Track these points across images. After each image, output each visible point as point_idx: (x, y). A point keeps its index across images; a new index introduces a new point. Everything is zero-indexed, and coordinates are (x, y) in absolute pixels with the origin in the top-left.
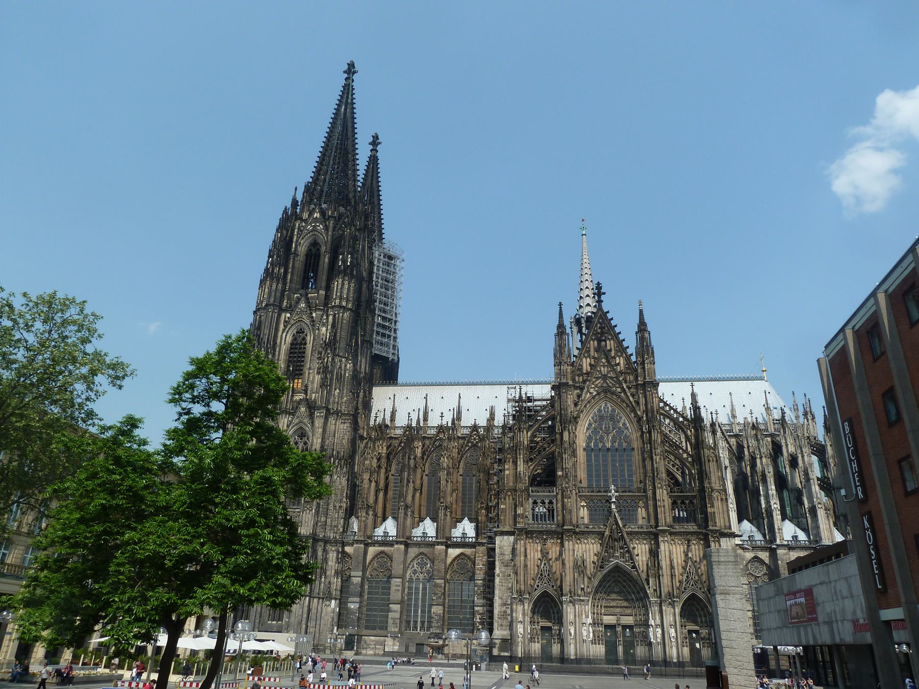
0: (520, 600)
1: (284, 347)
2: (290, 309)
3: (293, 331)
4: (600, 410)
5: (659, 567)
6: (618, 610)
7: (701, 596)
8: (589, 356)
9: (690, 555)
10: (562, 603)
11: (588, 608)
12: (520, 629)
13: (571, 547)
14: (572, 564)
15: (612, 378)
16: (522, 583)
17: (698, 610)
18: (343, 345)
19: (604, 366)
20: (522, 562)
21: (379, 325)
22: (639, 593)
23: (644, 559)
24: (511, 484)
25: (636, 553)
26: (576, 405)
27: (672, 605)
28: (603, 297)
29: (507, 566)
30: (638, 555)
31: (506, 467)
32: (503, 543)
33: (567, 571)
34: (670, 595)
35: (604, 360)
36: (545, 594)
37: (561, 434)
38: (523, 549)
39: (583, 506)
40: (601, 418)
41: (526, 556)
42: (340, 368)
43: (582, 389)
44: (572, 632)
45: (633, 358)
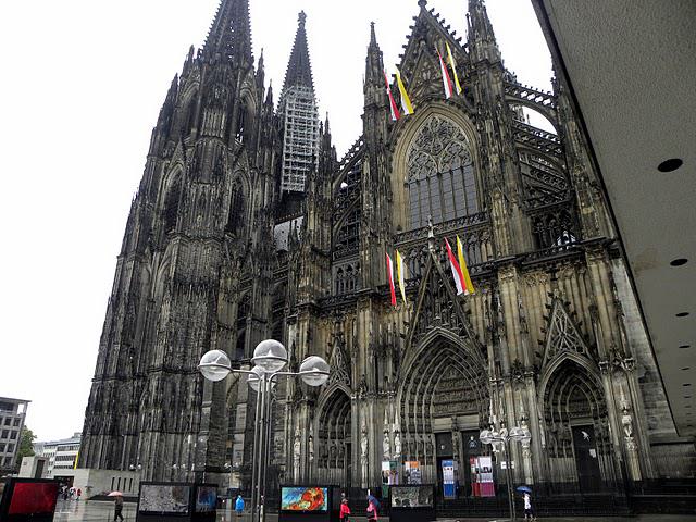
1: (164, 192)
2: (169, 157)
3: (172, 175)
4: (426, 129)
6: (456, 407)
7: (580, 361)
11: (394, 408)
12: (297, 449)
13: (368, 318)
17: (588, 391)
18: (206, 173)
21: (294, 164)
33: (362, 356)
38: (305, 334)
42: (203, 194)
44: (364, 447)
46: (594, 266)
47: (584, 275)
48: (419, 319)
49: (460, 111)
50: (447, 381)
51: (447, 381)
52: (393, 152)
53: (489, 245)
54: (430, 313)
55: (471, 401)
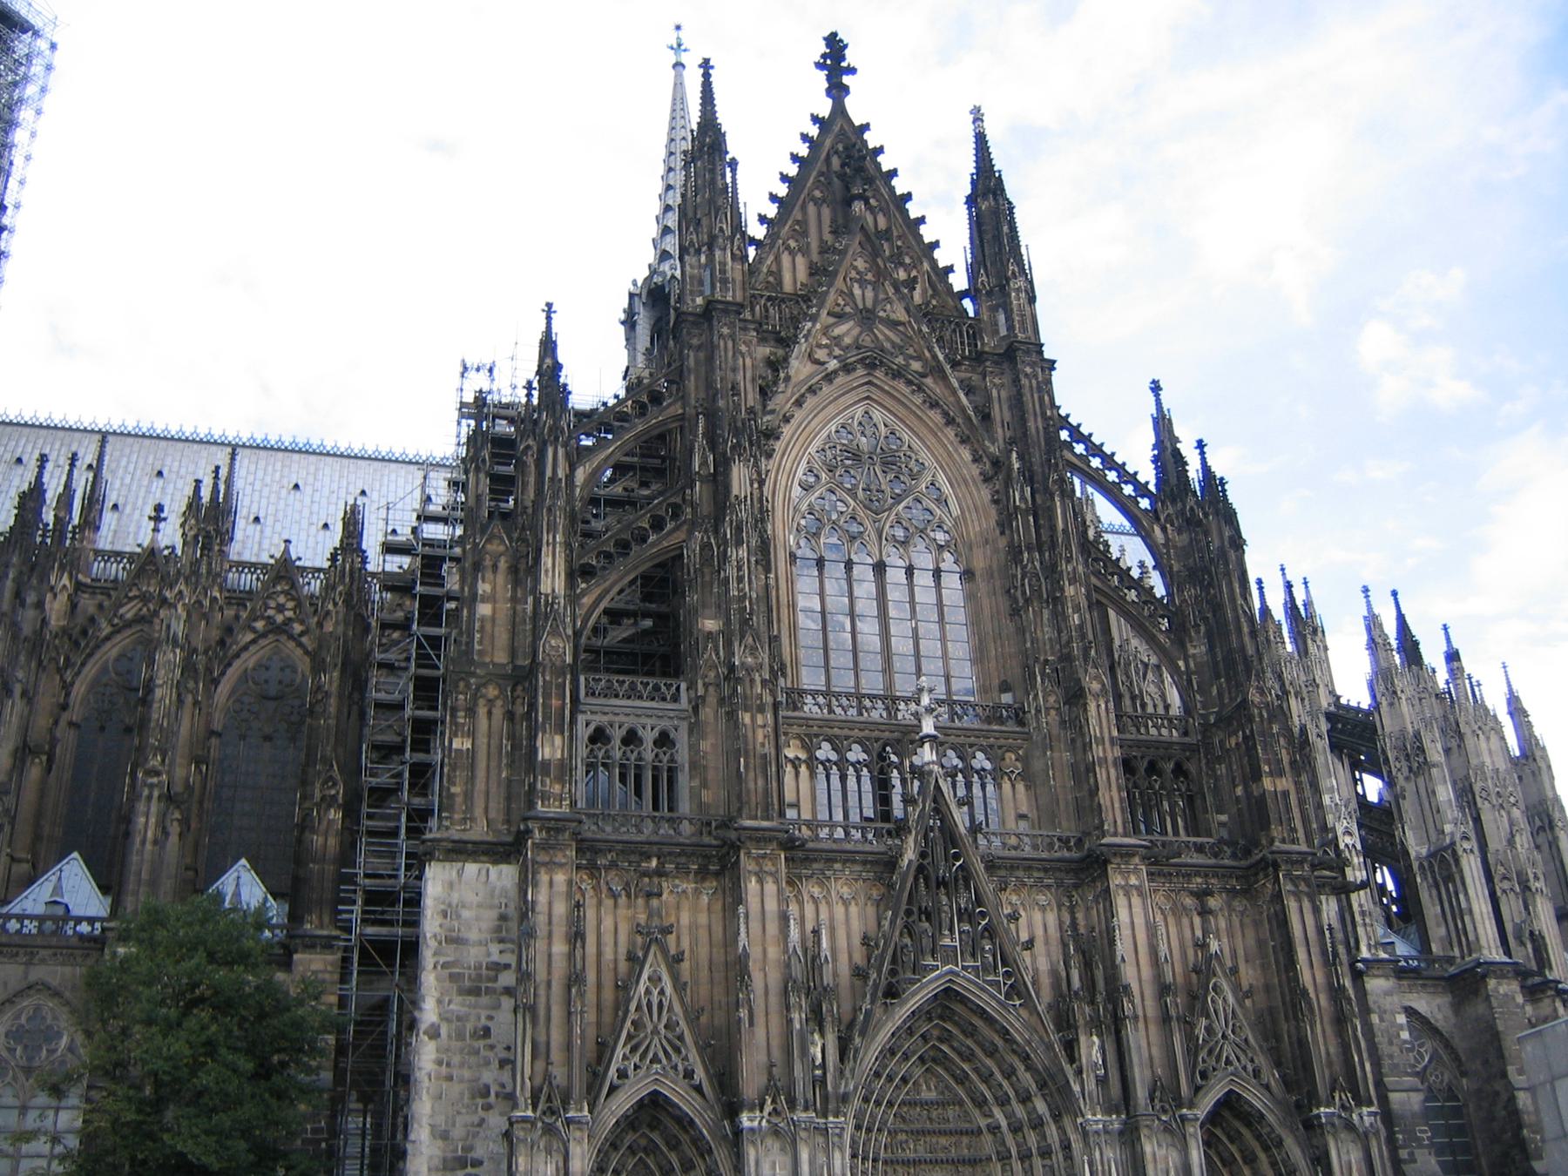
0: (549, 1130)
5: (1116, 990)
7: (1256, 1098)
8: (804, 250)
9: (1214, 946)
10: (736, 1139)
13: (772, 905)
14: (775, 977)
15: (894, 324)
16: (556, 1055)
19: (862, 283)
20: (560, 966)
22: (1025, 1099)
23: (1043, 965)
24: (501, 657)
25: (1024, 937)
26: (765, 393)
27: (1176, 1133)
28: (846, 79)
29: (475, 991)
30: (1029, 945)
31: (483, 588)
32: (456, 897)
34: (1168, 1095)
35: (860, 264)
36: (653, 1107)
37: (719, 480)
38: (560, 908)
39: (795, 763)
40: (846, 458)
41: (576, 936)
43: (787, 343)
45: (959, 281)
46: (1292, 905)
47: (1242, 913)
48: (901, 934)
49: (950, 432)
50: (912, 1104)
51: (912, 1104)
52: (769, 456)
53: (1020, 787)
54: (927, 925)
55: (973, 1162)
